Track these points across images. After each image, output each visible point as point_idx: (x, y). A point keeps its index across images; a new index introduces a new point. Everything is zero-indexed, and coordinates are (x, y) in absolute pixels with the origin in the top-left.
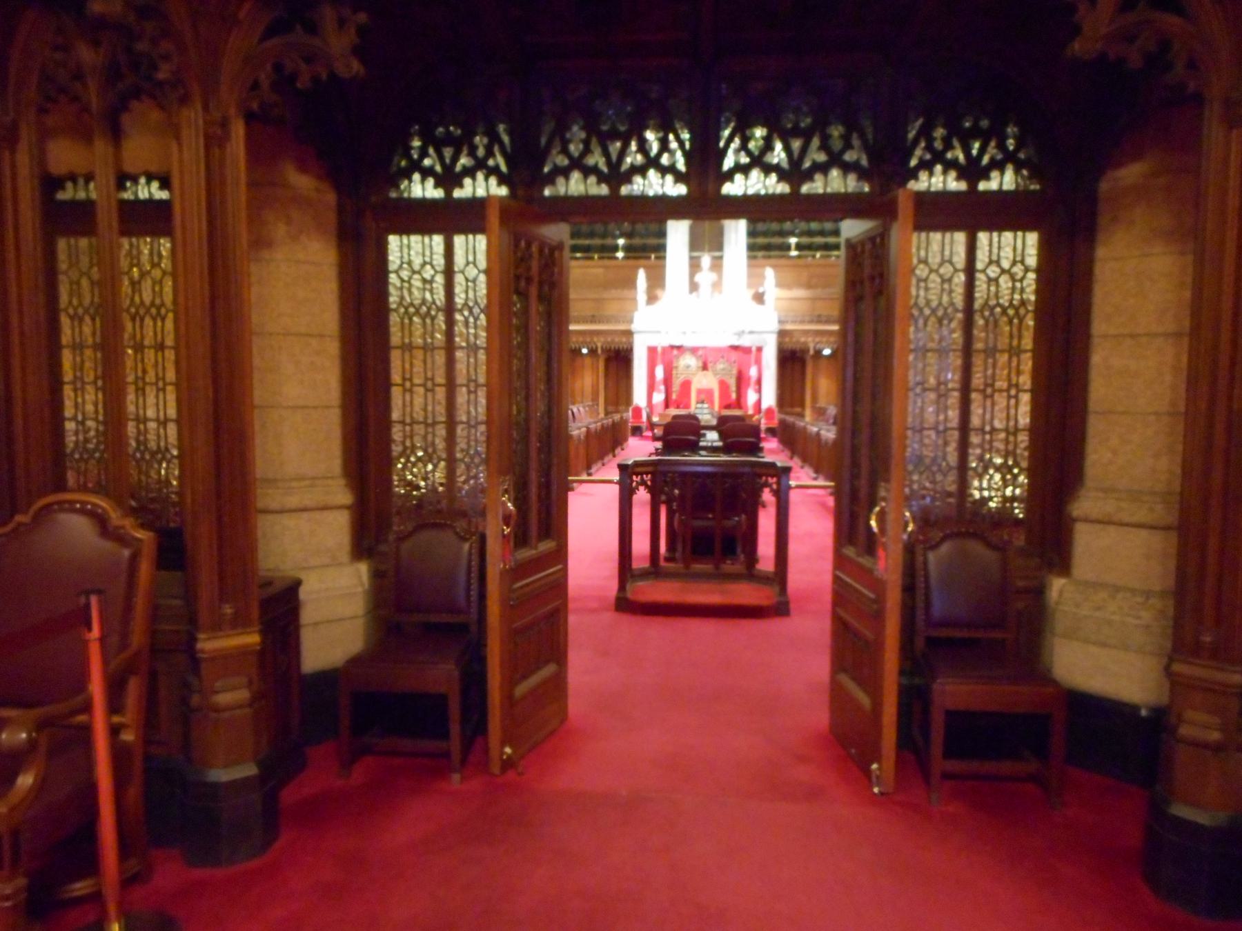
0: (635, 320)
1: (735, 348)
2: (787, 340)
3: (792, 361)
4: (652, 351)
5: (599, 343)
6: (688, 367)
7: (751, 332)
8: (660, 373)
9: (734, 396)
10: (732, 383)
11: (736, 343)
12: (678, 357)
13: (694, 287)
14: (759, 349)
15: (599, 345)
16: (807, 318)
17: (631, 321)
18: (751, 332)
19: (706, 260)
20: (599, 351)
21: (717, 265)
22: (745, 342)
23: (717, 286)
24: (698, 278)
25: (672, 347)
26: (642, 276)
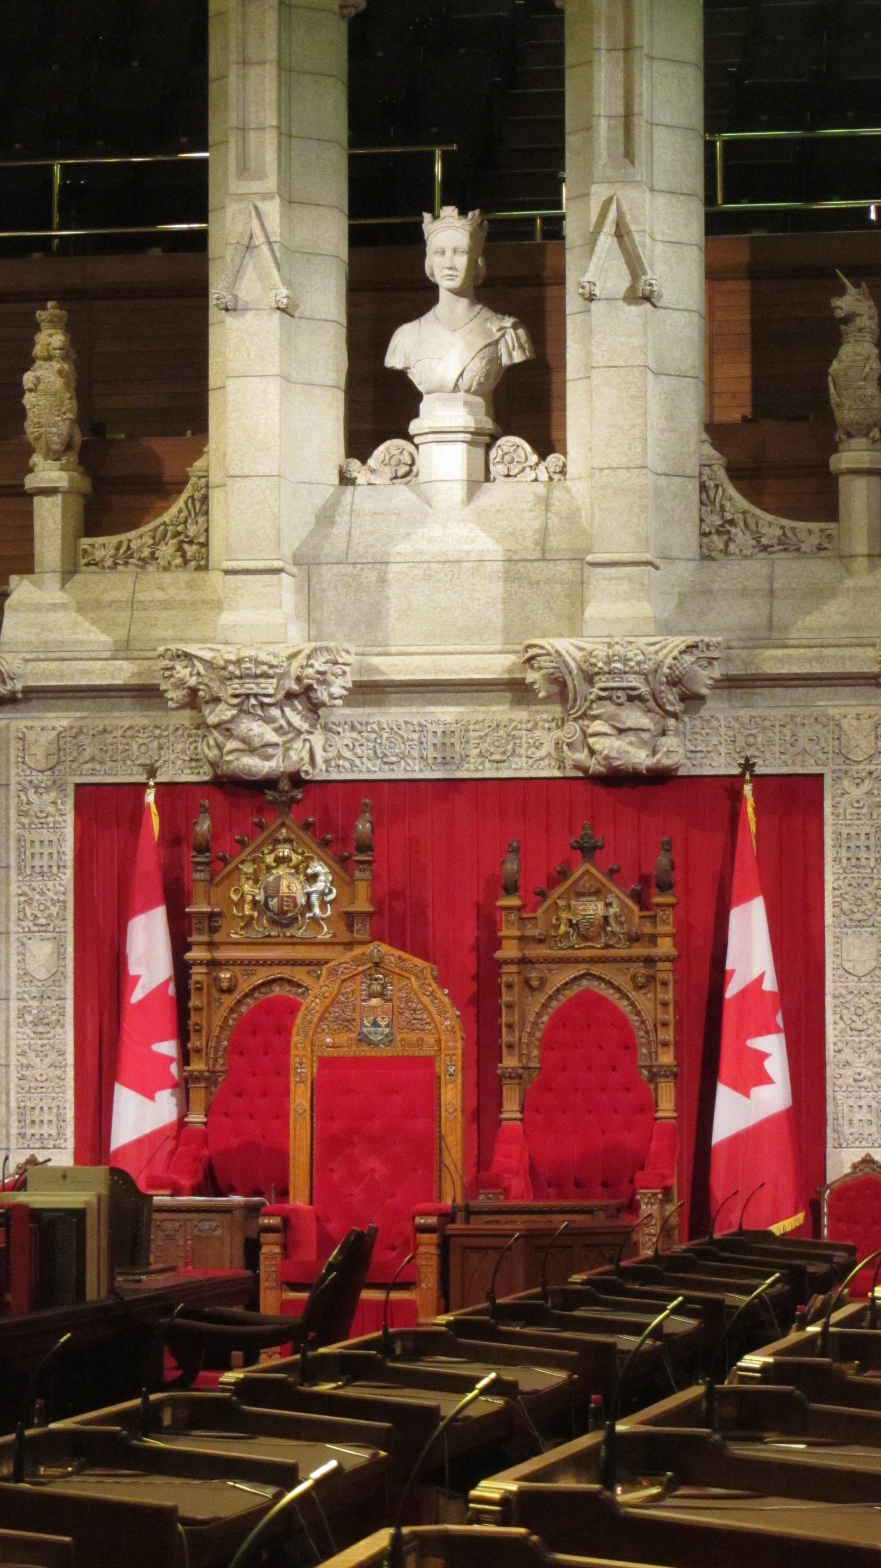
11: (640, 758)
13: (380, 407)
18: (733, 684)
19: (448, 240)
21: (521, 280)
23: (525, 404)
26: (50, 339)
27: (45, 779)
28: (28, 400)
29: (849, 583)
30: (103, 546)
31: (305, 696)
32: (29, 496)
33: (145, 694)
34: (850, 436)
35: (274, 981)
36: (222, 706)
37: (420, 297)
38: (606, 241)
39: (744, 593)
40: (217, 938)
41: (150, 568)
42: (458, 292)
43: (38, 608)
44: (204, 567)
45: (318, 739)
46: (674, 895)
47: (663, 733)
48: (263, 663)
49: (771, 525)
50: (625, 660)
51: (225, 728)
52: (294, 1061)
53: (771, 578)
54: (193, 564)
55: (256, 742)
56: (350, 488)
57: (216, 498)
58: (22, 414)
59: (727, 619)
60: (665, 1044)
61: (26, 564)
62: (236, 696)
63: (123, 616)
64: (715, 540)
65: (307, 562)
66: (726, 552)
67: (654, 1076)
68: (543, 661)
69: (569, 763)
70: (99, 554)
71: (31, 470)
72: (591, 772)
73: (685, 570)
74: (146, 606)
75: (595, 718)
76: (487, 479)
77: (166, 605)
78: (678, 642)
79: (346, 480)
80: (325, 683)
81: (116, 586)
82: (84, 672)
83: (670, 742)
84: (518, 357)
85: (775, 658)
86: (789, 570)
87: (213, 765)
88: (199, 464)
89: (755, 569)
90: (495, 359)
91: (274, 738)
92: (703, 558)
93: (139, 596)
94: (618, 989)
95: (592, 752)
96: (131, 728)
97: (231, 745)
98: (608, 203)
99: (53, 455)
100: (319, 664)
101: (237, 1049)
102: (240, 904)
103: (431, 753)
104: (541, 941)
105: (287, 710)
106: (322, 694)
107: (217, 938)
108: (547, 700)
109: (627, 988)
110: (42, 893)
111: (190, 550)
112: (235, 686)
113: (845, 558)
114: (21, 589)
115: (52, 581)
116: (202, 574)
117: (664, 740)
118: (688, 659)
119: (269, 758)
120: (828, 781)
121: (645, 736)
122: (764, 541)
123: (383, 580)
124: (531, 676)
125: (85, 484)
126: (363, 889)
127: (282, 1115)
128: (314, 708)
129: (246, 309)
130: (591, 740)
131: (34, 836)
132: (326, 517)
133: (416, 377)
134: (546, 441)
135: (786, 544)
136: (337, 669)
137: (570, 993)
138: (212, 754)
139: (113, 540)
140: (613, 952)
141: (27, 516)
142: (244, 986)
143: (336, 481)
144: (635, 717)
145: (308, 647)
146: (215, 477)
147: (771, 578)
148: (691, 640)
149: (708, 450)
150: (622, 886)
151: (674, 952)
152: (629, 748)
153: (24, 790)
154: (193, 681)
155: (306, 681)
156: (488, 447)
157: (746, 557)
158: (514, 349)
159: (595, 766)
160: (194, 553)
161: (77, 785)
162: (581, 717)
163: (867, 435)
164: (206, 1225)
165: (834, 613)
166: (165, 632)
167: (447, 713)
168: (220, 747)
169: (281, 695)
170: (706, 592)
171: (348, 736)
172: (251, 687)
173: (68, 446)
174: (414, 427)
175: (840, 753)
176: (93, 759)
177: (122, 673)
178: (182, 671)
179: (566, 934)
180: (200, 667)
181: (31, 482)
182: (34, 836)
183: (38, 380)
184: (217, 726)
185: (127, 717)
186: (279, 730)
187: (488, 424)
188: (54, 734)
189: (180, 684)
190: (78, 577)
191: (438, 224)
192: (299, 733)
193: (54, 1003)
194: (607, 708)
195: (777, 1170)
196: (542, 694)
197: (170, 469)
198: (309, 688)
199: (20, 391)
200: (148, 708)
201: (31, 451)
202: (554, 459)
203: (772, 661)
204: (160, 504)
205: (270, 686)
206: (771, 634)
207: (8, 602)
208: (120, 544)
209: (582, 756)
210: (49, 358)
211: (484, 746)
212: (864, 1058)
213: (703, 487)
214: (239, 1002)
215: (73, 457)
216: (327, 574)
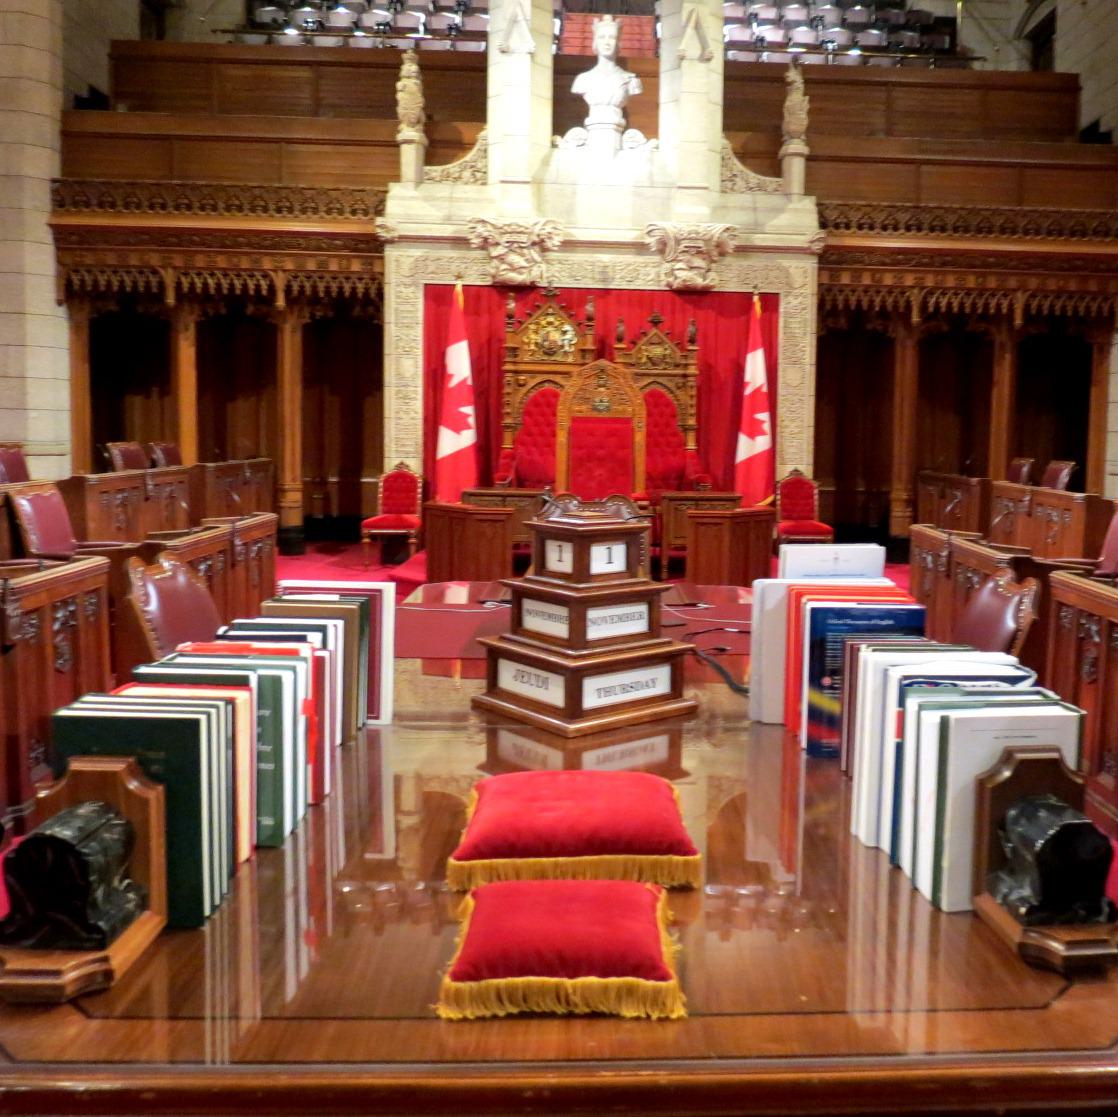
0: (391, 206)
1: (691, 296)
2: (845, 279)
3: (851, 343)
4: (437, 296)
5: (279, 273)
6: (550, 351)
7: (743, 250)
8: (459, 362)
9: (691, 445)
10: (686, 400)
11: (699, 282)
12: (518, 322)
13: (568, 112)
14: (770, 301)
15: (280, 281)
16: (903, 217)
17: (380, 212)
18: (743, 250)
20: (281, 302)
22: (728, 279)
23: (640, 114)
24: (581, 84)
25: (503, 289)
27: (407, 281)
28: (400, 96)
29: (791, 206)
30: (436, 171)
31: (540, 245)
32: (396, 145)
33: (459, 242)
34: (792, 138)
35: (545, 381)
36: (500, 247)
37: (588, 62)
38: (690, 31)
39: (742, 208)
40: (517, 359)
41: (459, 183)
42: (609, 58)
43: (403, 198)
44: (484, 184)
45: (544, 266)
46: (698, 346)
47: (709, 270)
48: (521, 226)
49: (754, 178)
50: (697, 233)
51: (501, 258)
52: (559, 419)
53: (755, 203)
54: (480, 182)
55: (516, 266)
56: (556, 150)
57: (491, 150)
58: (395, 103)
59: (738, 219)
60: (691, 415)
61: (397, 178)
62: (508, 242)
63: (446, 204)
64: (728, 184)
65: (537, 182)
66: (732, 189)
67: (686, 429)
68: (657, 233)
69: (664, 283)
70: (434, 174)
71: (399, 132)
72: (675, 287)
73: (715, 196)
74: (459, 200)
75: (681, 261)
76: (621, 148)
77: (467, 200)
78: (722, 226)
79: (554, 145)
80: (550, 238)
81: (443, 190)
82: (430, 229)
83: (712, 275)
84: (637, 91)
85: (759, 238)
86: (764, 200)
87: (494, 277)
88: (483, 133)
89: (746, 199)
90: (627, 91)
91: (524, 264)
92: (723, 192)
93: (454, 195)
94: (669, 389)
95: (676, 278)
96: (451, 258)
97: (504, 266)
98: (691, 12)
99: (412, 125)
100: (548, 229)
101: (527, 413)
102: (528, 344)
103: (598, 276)
104: (634, 365)
105: (532, 251)
106: (549, 244)
107: (518, 359)
108: (653, 253)
109: (674, 389)
110: (407, 336)
111: (479, 175)
112: (506, 238)
113: (788, 195)
114: (395, 189)
115: (411, 185)
116: (484, 187)
117: (710, 273)
118: (726, 234)
119: (521, 274)
120: (782, 297)
121: (703, 271)
122: (751, 185)
123: (574, 193)
124: (648, 240)
125: (425, 141)
126: (590, 339)
127: (551, 446)
128: (544, 250)
129: (513, 53)
130: (676, 272)
131: (402, 308)
132: (546, 162)
133: (588, 99)
134: (651, 130)
135: (761, 188)
136: (557, 232)
137: (663, 390)
138: (493, 271)
139: (439, 168)
140: (666, 371)
141: (397, 156)
142: (532, 383)
143: (549, 145)
144: (698, 262)
145: (543, 220)
146: (490, 140)
147: (755, 203)
148: (728, 225)
149: (726, 142)
150: (672, 341)
151: (697, 372)
152: (695, 277)
153: (398, 285)
154: (486, 234)
155: (541, 237)
156: (623, 133)
157: (743, 192)
158: (635, 86)
159: (676, 284)
160: (480, 177)
161: (426, 285)
162: (672, 261)
163: (799, 138)
164: (522, 504)
165: (783, 220)
166: (470, 212)
167: (605, 258)
168: (497, 268)
169: (529, 244)
170: (724, 207)
171: (557, 267)
172: (514, 238)
173: (418, 122)
174: (587, 121)
175: (787, 284)
176: (433, 273)
177: (448, 231)
178: (480, 229)
179: (645, 363)
180: (490, 228)
181: (400, 137)
182: (402, 308)
183: (405, 86)
184: (496, 257)
185: (448, 253)
186: (527, 260)
187: (623, 122)
188: (413, 259)
189: (479, 236)
190: (424, 185)
191: (602, 23)
192: (537, 262)
193: (412, 389)
194: (686, 257)
195: (760, 474)
196: (653, 249)
197: (466, 138)
198: (543, 241)
199: (394, 91)
200: (460, 249)
201: (400, 123)
202: (653, 142)
203: (759, 240)
204: (461, 154)
205: (523, 238)
206: (757, 228)
207: (389, 195)
208: (443, 171)
209: (671, 279)
210: (409, 77)
211: (623, 274)
212: (795, 424)
213: (723, 159)
214: (528, 392)
215: (420, 127)
216: (547, 189)
